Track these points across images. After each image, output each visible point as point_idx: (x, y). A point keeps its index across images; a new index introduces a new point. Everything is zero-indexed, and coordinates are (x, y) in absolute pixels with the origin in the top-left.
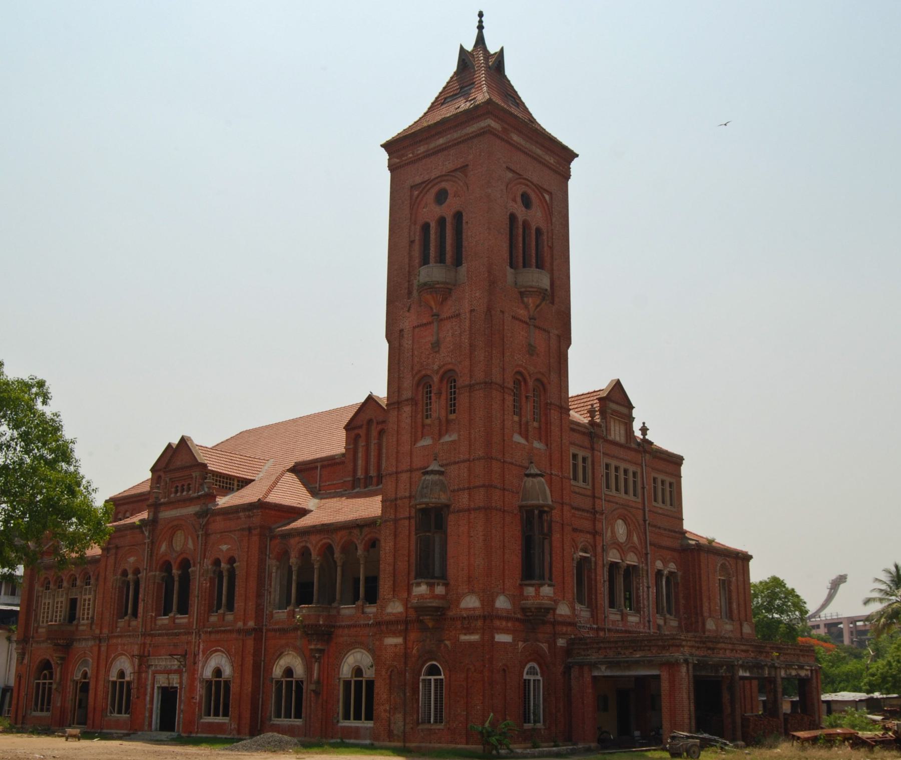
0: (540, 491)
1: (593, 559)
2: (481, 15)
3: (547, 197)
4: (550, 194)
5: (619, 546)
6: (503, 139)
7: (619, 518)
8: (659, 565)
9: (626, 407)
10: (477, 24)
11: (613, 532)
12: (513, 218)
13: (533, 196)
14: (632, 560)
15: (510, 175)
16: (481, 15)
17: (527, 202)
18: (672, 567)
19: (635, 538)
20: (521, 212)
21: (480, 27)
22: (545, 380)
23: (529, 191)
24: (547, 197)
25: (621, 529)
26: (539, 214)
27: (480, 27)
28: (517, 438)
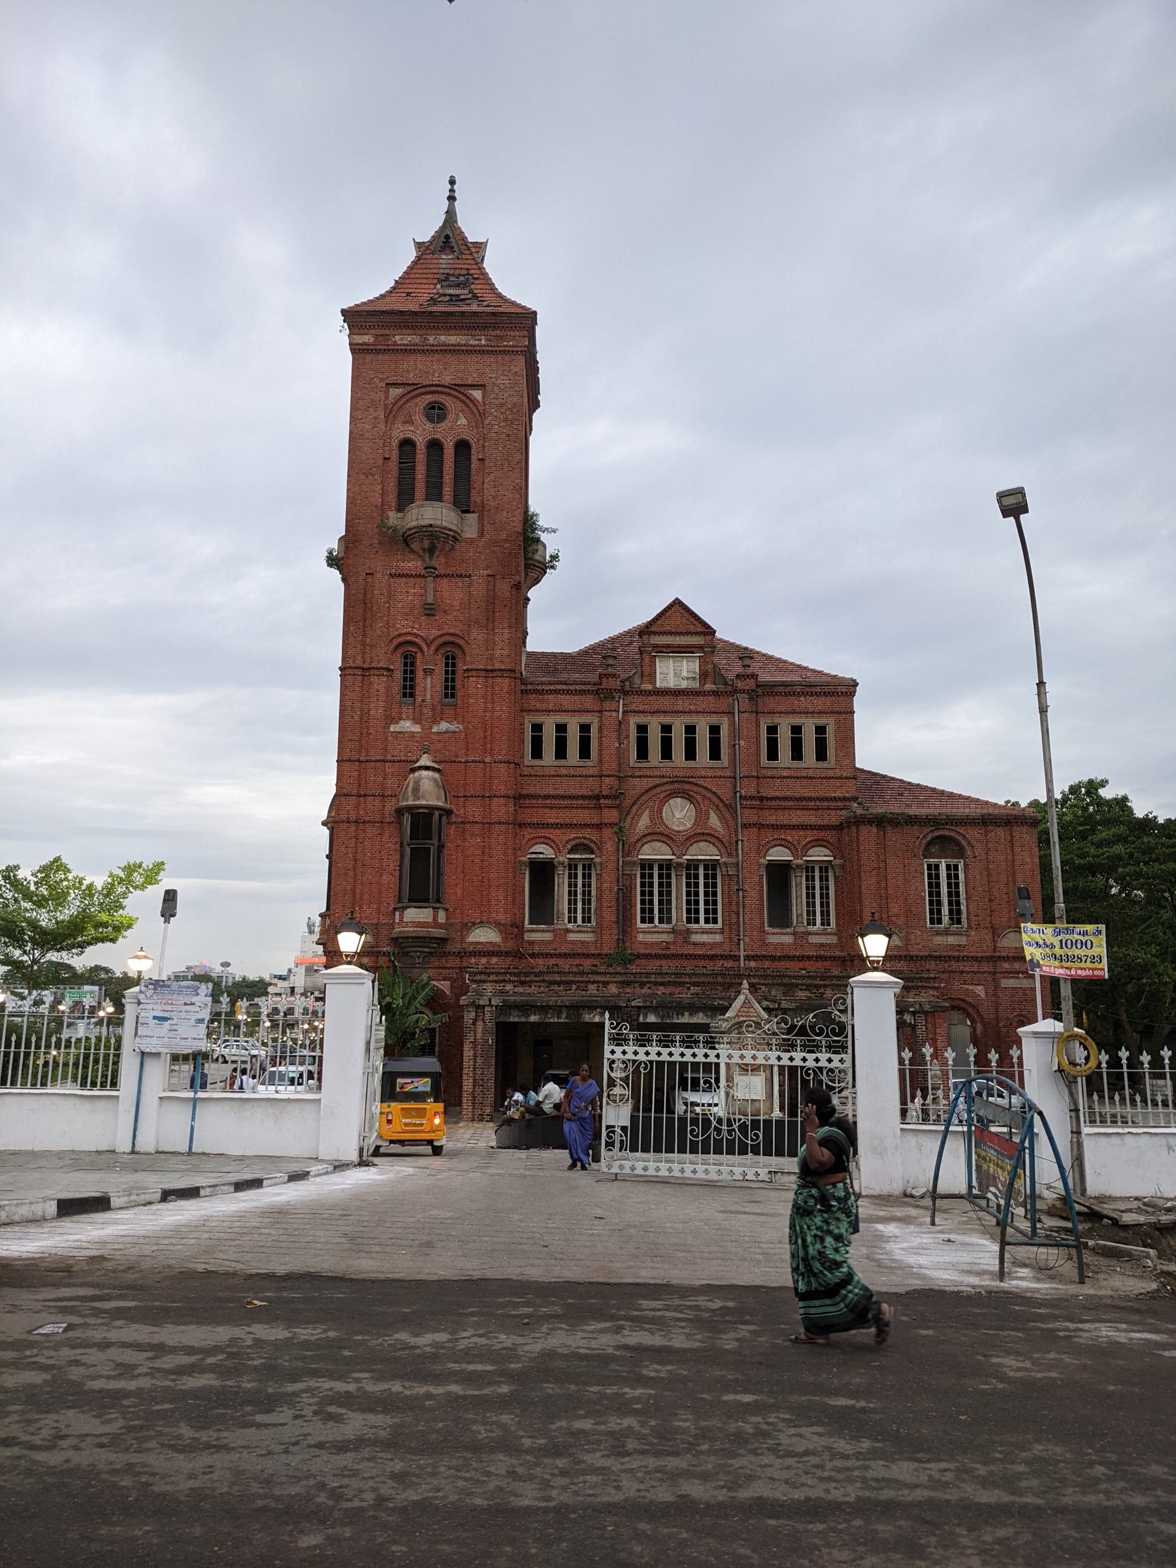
0: (427, 788)
1: (598, 860)
2: (452, 182)
3: (477, 394)
4: (481, 386)
5: (666, 836)
6: (378, 351)
7: (673, 794)
8: (779, 854)
9: (702, 633)
10: (448, 194)
11: (657, 816)
12: (407, 445)
13: (448, 402)
14: (704, 852)
15: (395, 392)
16: (452, 182)
17: (436, 412)
18: (820, 855)
19: (714, 821)
20: (421, 432)
21: (452, 199)
22: (462, 642)
23: (436, 398)
24: (477, 394)
25: (679, 814)
26: (463, 421)
27: (452, 199)
28: (407, 726)
